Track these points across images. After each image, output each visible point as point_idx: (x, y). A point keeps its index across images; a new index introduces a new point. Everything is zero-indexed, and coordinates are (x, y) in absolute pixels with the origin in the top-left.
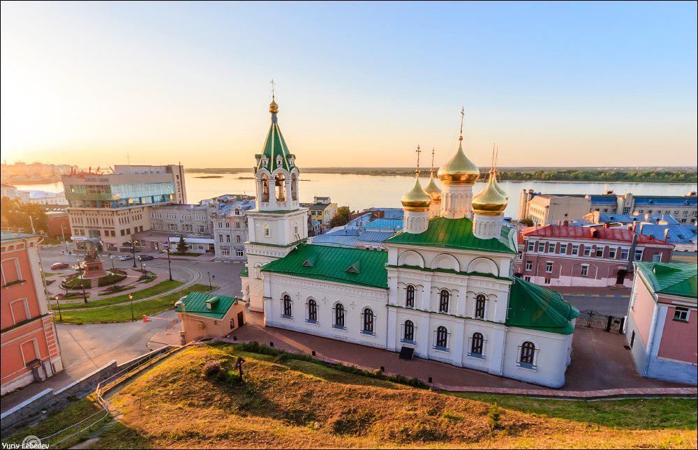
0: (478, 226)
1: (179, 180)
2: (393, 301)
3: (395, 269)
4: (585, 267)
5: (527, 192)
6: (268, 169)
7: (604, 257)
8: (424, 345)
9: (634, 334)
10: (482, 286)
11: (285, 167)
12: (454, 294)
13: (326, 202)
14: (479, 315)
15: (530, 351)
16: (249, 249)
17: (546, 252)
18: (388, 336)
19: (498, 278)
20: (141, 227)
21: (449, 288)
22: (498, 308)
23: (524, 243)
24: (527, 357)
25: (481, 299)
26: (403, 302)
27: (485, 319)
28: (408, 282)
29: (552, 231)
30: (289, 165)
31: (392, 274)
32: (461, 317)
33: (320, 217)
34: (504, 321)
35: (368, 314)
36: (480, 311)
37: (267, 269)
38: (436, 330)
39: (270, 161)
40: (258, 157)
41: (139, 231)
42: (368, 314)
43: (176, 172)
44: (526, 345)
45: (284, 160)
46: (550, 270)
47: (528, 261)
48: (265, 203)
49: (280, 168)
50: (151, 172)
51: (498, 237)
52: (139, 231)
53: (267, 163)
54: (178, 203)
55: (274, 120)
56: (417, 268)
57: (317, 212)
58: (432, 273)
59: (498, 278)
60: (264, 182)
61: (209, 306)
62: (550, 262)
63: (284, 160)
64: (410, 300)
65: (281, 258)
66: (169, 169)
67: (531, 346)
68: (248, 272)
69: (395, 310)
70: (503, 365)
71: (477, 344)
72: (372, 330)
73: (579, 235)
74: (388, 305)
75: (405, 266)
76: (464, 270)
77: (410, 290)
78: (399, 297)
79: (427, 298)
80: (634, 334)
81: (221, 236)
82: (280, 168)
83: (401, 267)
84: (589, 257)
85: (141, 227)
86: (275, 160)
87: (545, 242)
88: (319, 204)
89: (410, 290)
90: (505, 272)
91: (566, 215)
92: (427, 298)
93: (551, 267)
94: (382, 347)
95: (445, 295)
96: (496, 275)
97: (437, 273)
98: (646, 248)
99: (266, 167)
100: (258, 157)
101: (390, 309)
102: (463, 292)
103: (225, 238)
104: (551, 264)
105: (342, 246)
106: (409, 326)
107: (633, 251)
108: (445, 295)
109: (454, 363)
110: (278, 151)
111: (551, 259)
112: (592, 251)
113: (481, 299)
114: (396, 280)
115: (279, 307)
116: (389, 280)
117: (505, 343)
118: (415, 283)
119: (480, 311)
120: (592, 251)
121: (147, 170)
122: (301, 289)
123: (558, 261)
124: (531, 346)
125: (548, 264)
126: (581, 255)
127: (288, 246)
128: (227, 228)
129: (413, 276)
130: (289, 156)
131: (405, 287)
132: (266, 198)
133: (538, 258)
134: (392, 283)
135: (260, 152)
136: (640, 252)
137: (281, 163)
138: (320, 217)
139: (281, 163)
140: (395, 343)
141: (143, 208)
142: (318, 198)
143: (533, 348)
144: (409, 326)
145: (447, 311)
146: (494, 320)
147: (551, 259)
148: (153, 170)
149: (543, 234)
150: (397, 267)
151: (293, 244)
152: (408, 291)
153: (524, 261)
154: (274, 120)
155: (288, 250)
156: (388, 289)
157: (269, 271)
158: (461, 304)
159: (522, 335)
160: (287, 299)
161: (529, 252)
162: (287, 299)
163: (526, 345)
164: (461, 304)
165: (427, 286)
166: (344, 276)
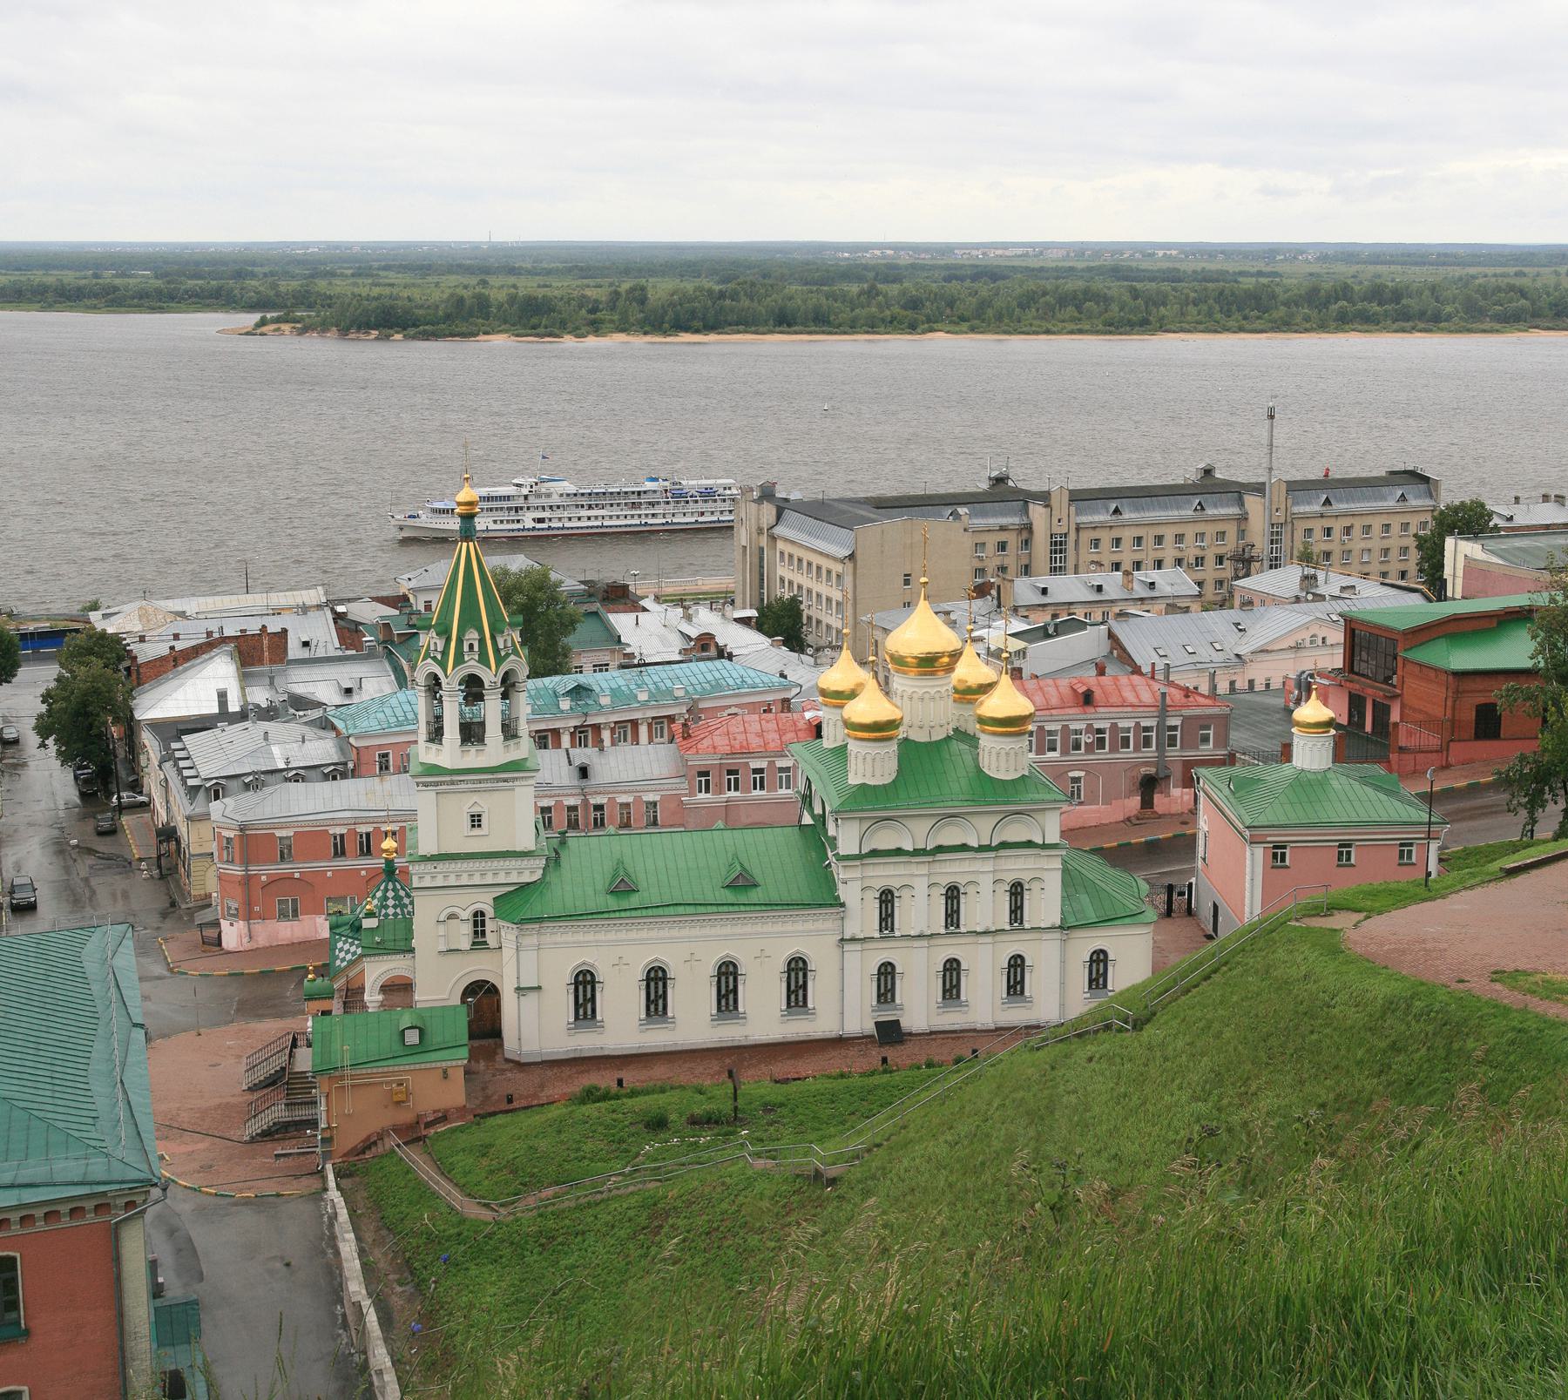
0: (994, 757)
3: (858, 863)
4: (1076, 780)
7: (1111, 751)
8: (919, 1008)
9: (1216, 907)
10: (1017, 866)
12: (971, 890)
16: (420, 876)
21: (961, 880)
22: (1045, 906)
24: (1097, 980)
25: (1017, 890)
26: (873, 928)
27: (1027, 926)
31: (840, 872)
35: (797, 971)
39: (482, 641)
58: (930, 859)
59: (1044, 846)
69: (858, 947)
70: (1062, 1005)
71: (1016, 975)
75: (875, 853)
76: (986, 842)
77: (887, 898)
78: (862, 916)
79: (920, 911)
80: (1216, 907)
84: (1080, 755)
86: (493, 638)
89: (887, 898)
90: (1053, 837)
91: (907, 582)
92: (920, 911)
94: (833, 1035)
97: (940, 857)
98: (1186, 719)
101: (847, 947)
102: (986, 883)
107: (1161, 727)
109: (979, 1027)
112: (1086, 739)
113: (1017, 890)
114: (857, 886)
115: (562, 1002)
116: (840, 886)
117: (1063, 962)
118: (894, 883)
120: (1086, 739)
126: (1065, 752)
129: (890, 870)
132: (472, 733)
136: (1174, 728)
140: (860, 1018)
144: (887, 972)
150: (860, 857)
152: (881, 903)
156: (843, 905)
158: (984, 907)
159: (1085, 944)
164: (984, 907)
165: (921, 885)
166: (729, 896)
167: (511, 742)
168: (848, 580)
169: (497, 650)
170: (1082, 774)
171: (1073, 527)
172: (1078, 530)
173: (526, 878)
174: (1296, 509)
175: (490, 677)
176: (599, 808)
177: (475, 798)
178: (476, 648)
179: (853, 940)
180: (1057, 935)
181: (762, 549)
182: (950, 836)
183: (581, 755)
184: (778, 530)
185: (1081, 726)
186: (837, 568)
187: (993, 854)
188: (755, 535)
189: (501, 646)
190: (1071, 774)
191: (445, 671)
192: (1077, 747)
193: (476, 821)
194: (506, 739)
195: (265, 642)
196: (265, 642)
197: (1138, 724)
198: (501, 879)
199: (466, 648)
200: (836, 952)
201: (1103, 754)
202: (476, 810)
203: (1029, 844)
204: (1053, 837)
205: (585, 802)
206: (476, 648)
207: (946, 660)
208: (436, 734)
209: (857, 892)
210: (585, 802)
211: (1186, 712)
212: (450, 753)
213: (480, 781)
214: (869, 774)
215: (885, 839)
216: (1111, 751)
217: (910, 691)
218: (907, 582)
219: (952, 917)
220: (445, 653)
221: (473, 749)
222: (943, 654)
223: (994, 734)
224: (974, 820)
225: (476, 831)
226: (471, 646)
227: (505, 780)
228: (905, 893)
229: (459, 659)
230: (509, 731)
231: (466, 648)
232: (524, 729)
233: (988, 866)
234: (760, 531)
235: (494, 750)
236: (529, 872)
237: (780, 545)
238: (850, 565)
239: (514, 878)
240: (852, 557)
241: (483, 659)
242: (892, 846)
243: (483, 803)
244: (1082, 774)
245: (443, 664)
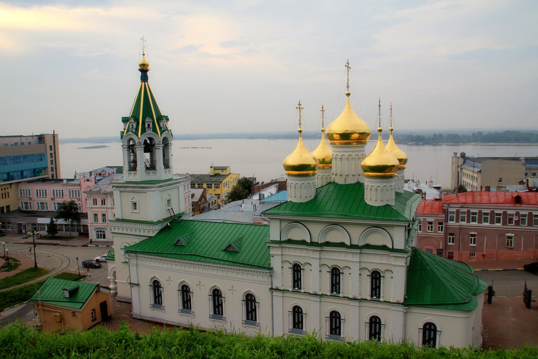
1: (53, 152)
2: (277, 284)
5: (459, 155)
7: (528, 226)
10: (376, 261)
12: (346, 271)
13: (225, 173)
14: (376, 296)
15: (432, 333)
17: (468, 222)
18: (274, 324)
19: (393, 250)
20: (8, 207)
21: (341, 265)
22: (395, 287)
25: (376, 277)
26: (288, 284)
28: (293, 260)
29: (473, 198)
30: (160, 128)
32: (355, 299)
33: (218, 191)
34: (402, 301)
35: (250, 300)
36: (376, 290)
37: (129, 251)
38: (328, 316)
40: (125, 120)
41: (5, 211)
42: (250, 300)
43: (49, 142)
44: (428, 327)
46: (474, 243)
47: (450, 233)
48: (133, 173)
49: (149, 132)
50: (22, 143)
51: (392, 203)
52: (5, 211)
53: (135, 127)
54: (50, 178)
55: (144, 78)
56: (303, 242)
57: (213, 185)
58: (319, 249)
59: (393, 250)
60: (131, 148)
61: (67, 295)
62: (473, 233)
64: (297, 282)
65: (151, 237)
66: (41, 138)
67: (433, 327)
68: (114, 255)
69: (280, 294)
72: (256, 320)
73: (501, 200)
74: (271, 289)
75: (290, 241)
76: (355, 242)
77: (297, 269)
79: (315, 279)
81: (96, 215)
82: (149, 132)
84: (512, 226)
85: (8, 207)
86: (143, 123)
87: (465, 210)
88: (216, 175)
89: (297, 269)
91: (500, 181)
92: (315, 279)
93: (474, 239)
95: (335, 273)
96: (391, 247)
99: (134, 131)
100: (125, 120)
101: (275, 293)
102: (355, 269)
103: (100, 217)
104: (474, 235)
105: (226, 222)
106: (297, 312)
108: (335, 273)
110: (147, 112)
111: (475, 230)
112: (515, 218)
113: (376, 277)
118: (301, 261)
119: (376, 290)
120: (515, 218)
121: (17, 140)
122: (172, 274)
123: (482, 232)
124: (433, 327)
125: (472, 235)
126: (504, 224)
127: (159, 222)
128: (103, 206)
130: (160, 118)
131: (291, 266)
133: (461, 228)
134: (276, 263)
135: (128, 113)
137: (151, 126)
138: (218, 191)
139: (151, 126)
141: (11, 184)
142: (216, 169)
143: (435, 330)
145: (339, 293)
146: (392, 301)
147: (475, 230)
148: (23, 140)
149: (463, 201)
150: (280, 242)
151: (165, 220)
153: (446, 234)
154: (144, 78)
155: (158, 228)
156: (271, 269)
157: (135, 252)
158: (355, 284)
159: (421, 316)
160: (156, 285)
161: (450, 223)
162: (156, 285)
163: (428, 327)
164: (355, 284)
166: (223, 255)
168: (479, 179)
170: (513, 235)
173: (152, 234)
177: (133, 195)
179: (277, 290)
180: (401, 308)
181: (458, 172)
185: (514, 212)
186: (476, 175)
187: (358, 251)
189: (146, 126)
190: (507, 234)
192: (511, 220)
198: (142, 233)
200: (270, 294)
201: (524, 227)
202: (134, 200)
203: (384, 248)
204: (399, 244)
209: (280, 261)
213: (135, 187)
214: (293, 196)
216: (528, 226)
217: (340, 154)
219: (335, 286)
222: (355, 133)
223: (371, 177)
224: (348, 228)
225: (135, 211)
226: (133, 125)
227: (144, 188)
228: (388, 275)
231: (131, 127)
233: (356, 258)
234: (458, 167)
237: (464, 171)
239: (146, 234)
240: (480, 171)
242: (300, 239)
243: (137, 198)
244: (513, 235)
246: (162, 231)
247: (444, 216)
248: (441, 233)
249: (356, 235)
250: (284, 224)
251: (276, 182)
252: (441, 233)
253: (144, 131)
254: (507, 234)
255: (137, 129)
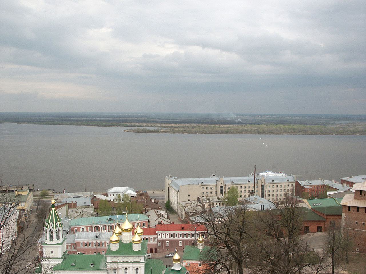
6: (53, 228)
11: (60, 226)
12: (129, 269)
19: (141, 262)
23: (157, 235)
25: (137, 269)
39: (53, 224)
45: (59, 223)
59: (141, 262)
62: (167, 241)
63: (59, 223)
75: (112, 262)
76: (131, 261)
83: (111, 262)
84: (181, 238)
86: (55, 224)
91: (189, 196)
97: (123, 263)
102: (131, 268)
113: (137, 269)
139: (58, 224)
150: (110, 263)
153: (157, 243)
155: (62, 260)
167: (58, 240)
169: (56, 225)
170: (182, 241)
171: (224, 185)
172: (225, 185)
174: (267, 182)
175: (55, 230)
176: (99, 243)
177: (52, 249)
178: (52, 225)
182: (125, 260)
183: (97, 233)
184: (172, 185)
186: (176, 192)
187: (132, 263)
188: (167, 185)
189: (57, 225)
191: (47, 229)
193: (52, 252)
194: (57, 239)
195: (73, 204)
196: (73, 204)
197: (191, 233)
199: (51, 225)
202: (52, 251)
203: (139, 262)
205: (97, 242)
206: (52, 225)
207: (129, 230)
208: (46, 239)
210: (97, 242)
211: (200, 232)
212: (48, 242)
215: (115, 260)
216: (187, 237)
218: (189, 196)
220: (48, 226)
221: (52, 241)
222: (129, 229)
229: (50, 227)
230: (58, 238)
231: (51, 225)
232: (61, 238)
234: (168, 185)
235: (55, 241)
236: (61, 261)
238: (178, 192)
240: (179, 191)
241: (53, 228)
244: (182, 241)
245: (47, 228)
246: (63, 261)
247: (157, 235)
248: (156, 243)
249: (131, 259)
250: (111, 257)
251: (66, 204)
252: (156, 243)
253: (56, 227)
254: (179, 241)
255: (53, 226)
